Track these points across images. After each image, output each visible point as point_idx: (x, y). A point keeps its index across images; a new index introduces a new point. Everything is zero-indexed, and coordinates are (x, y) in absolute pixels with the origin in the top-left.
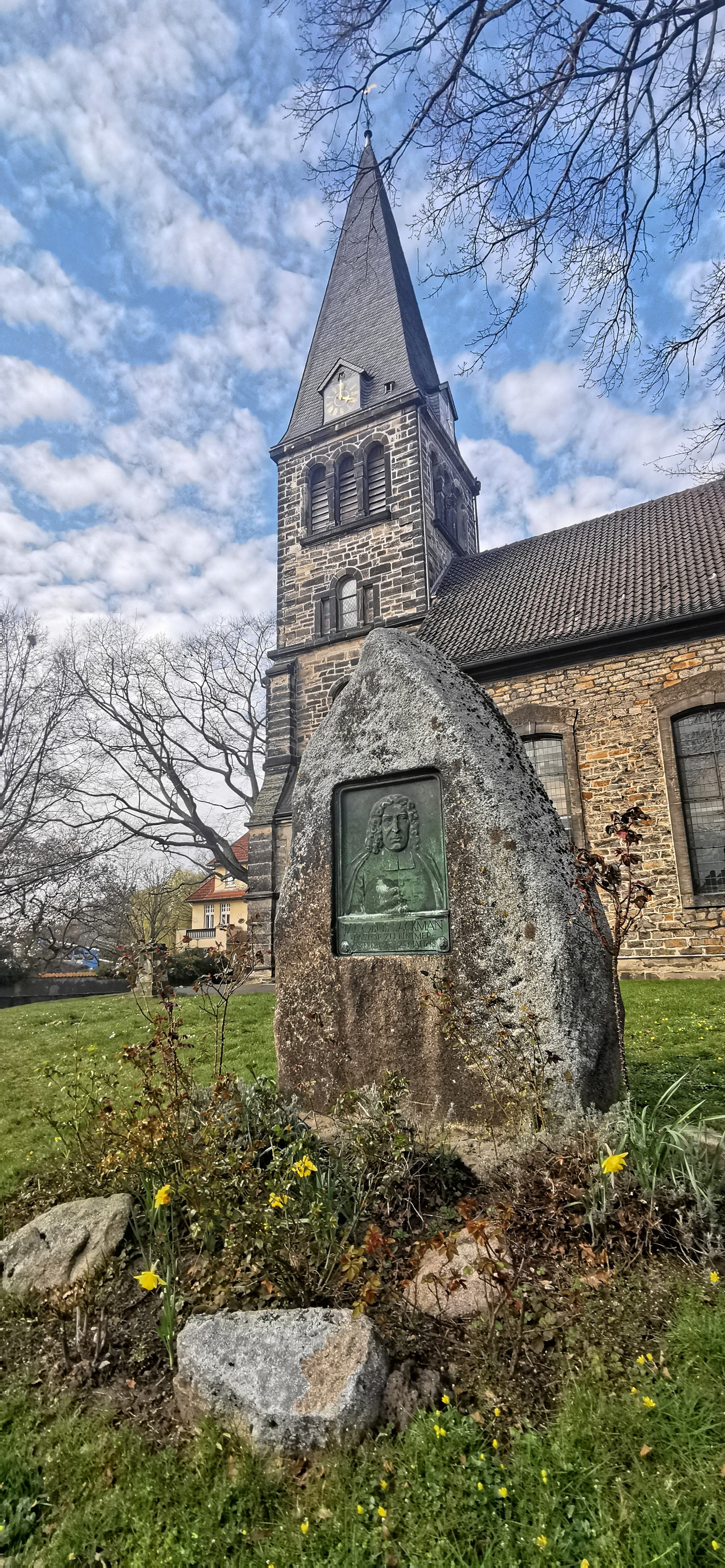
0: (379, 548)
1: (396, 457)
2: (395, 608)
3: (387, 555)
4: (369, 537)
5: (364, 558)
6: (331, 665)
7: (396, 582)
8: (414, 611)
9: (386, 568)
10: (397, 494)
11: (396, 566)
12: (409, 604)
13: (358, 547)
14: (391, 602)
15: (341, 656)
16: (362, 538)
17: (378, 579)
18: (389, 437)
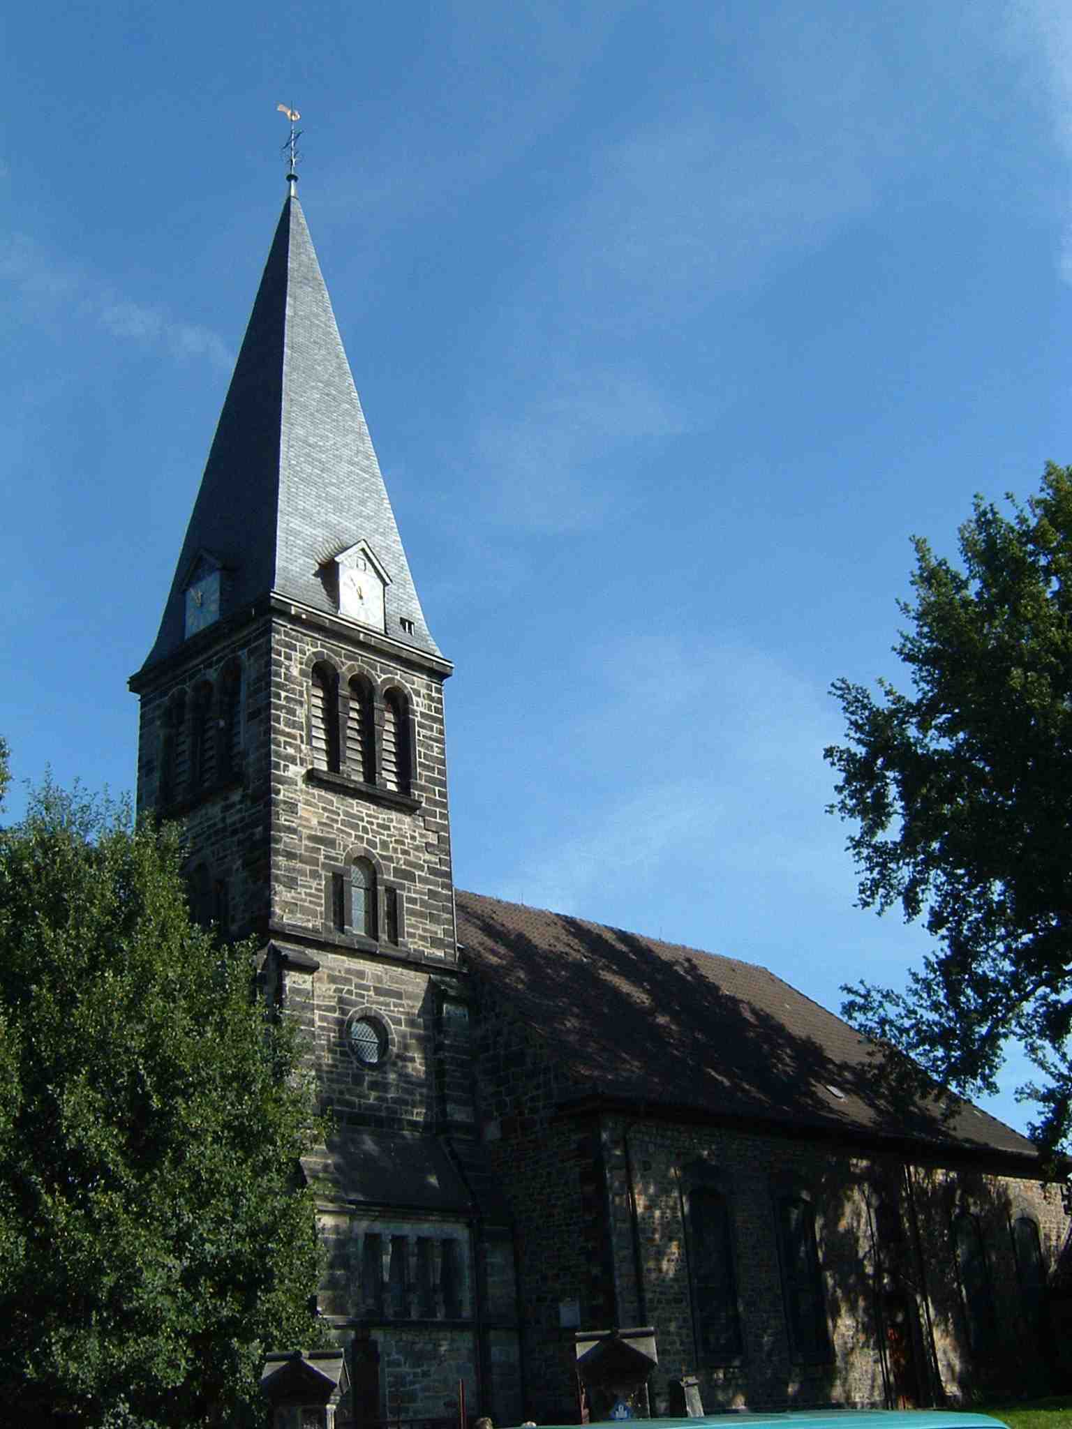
0: (403, 843)
1: (423, 732)
2: (423, 938)
3: (411, 858)
4: (392, 821)
5: (385, 845)
6: (348, 981)
7: (423, 903)
8: (440, 953)
9: (410, 877)
10: (423, 783)
11: (424, 880)
12: (436, 943)
13: (379, 825)
14: (418, 928)
15: (361, 974)
16: (384, 815)
17: (402, 887)
18: (415, 698)
